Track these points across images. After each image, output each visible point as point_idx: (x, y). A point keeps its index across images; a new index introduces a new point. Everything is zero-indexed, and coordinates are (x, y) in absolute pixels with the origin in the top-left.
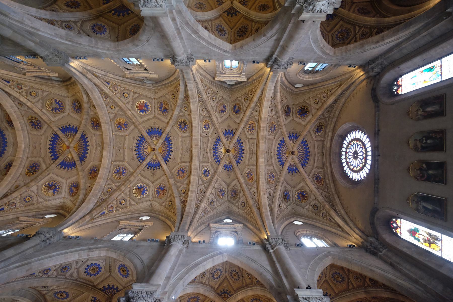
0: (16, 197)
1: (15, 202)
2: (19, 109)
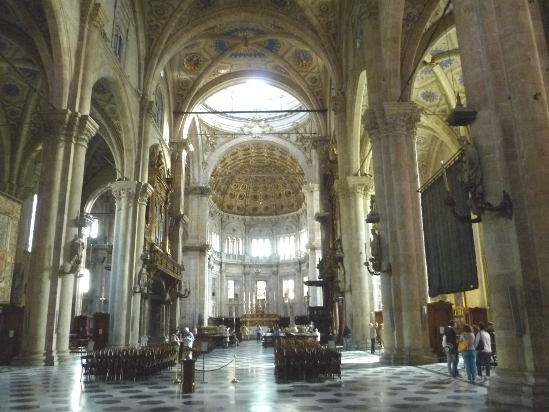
0: (319, 21)
1: (325, 22)
2: (188, 24)
